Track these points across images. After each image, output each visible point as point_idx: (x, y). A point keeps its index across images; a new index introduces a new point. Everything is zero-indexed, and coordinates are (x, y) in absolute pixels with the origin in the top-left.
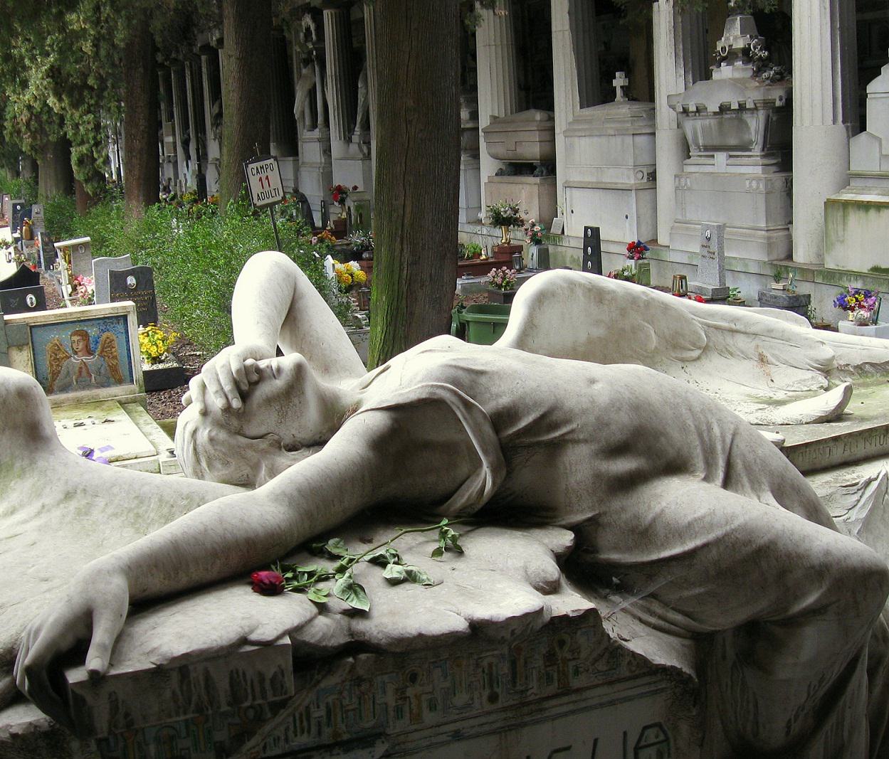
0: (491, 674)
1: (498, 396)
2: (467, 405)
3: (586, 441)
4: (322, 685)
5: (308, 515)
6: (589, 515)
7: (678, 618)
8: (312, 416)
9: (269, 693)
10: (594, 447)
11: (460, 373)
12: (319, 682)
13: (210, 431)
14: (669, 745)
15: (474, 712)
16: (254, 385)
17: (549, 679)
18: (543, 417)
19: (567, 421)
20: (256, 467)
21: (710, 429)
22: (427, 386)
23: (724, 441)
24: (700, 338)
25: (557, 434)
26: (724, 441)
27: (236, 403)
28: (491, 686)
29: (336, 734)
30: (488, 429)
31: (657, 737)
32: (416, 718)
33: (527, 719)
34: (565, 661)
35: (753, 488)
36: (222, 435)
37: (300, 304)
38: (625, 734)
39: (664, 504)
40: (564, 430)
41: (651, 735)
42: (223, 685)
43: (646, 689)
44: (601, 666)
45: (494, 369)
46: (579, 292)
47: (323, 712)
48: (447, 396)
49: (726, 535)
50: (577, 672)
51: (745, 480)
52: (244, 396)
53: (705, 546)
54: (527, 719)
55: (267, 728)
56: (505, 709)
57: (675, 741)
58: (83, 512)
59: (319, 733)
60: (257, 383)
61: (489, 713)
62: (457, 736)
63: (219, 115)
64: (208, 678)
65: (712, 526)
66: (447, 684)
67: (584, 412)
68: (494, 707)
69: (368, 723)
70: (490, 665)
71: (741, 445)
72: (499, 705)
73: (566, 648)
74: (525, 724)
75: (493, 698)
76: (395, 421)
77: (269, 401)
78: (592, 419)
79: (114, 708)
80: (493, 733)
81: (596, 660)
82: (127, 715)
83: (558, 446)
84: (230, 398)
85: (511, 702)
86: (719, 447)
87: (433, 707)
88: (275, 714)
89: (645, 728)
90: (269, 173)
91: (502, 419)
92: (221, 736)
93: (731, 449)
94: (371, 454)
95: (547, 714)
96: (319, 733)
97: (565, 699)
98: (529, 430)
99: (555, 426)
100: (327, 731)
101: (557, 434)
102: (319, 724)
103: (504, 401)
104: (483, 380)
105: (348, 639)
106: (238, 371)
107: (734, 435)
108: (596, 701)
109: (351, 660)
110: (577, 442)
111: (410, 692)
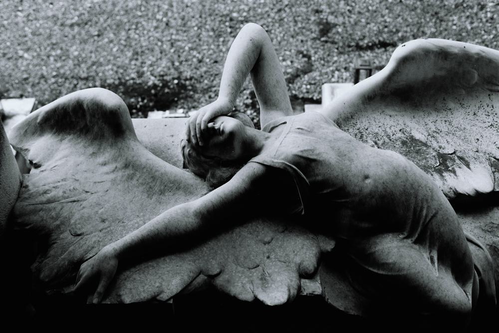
1: (317, 175)
8: (237, 150)
11: (302, 160)
13: (189, 151)
20: (207, 171)
21: (421, 210)
22: (284, 163)
36: (194, 154)
39: (377, 249)
45: (321, 159)
51: (428, 242)
58: (130, 177)
65: (391, 270)
67: (355, 195)
78: (357, 199)
84: (199, 140)
104: (313, 164)
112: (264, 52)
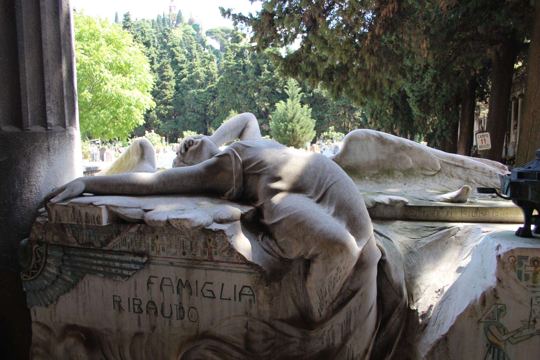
0: (183, 244)
2: (236, 157)
3: (267, 174)
4: (130, 231)
5: (164, 183)
6: (261, 203)
7: (277, 249)
9: (96, 222)
10: (269, 176)
12: (129, 229)
14: (254, 297)
15: (177, 257)
16: (190, 146)
17: (205, 253)
18: (258, 164)
19: (265, 166)
23: (327, 185)
24: (437, 166)
25: (261, 170)
26: (327, 185)
27: (183, 151)
28: (183, 248)
29: (133, 250)
30: (239, 166)
31: (249, 292)
32: (158, 252)
33: (196, 266)
34: (211, 248)
35: (329, 204)
37: (246, 129)
38: (235, 286)
40: (263, 169)
41: (246, 291)
42: (84, 216)
43: (244, 270)
44: (225, 254)
45: (254, 146)
46: (373, 139)
47: (130, 241)
48: (230, 153)
49: (290, 216)
50: (216, 254)
51: (328, 201)
52: (186, 149)
53: (283, 219)
54: (196, 266)
55: (115, 241)
56: (188, 259)
57: (257, 297)
59: (129, 247)
60: (192, 145)
61: (182, 259)
62: (172, 264)
63: (516, 125)
64: (80, 212)
66: (169, 243)
67: (272, 164)
68: (183, 257)
69: (143, 249)
70: (183, 241)
71: (334, 186)
72: (186, 257)
73: (211, 243)
74: (195, 268)
75: (184, 254)
76: (218, 161)
77: (191, 151)
79: (57, 215)
80: (184, 267)
81: (223, 251)
82: (60, 217)
83: (259, 175)
85: (190, 257)
86: (325, 186)
87: (164, 250)
88: (117, 237)
89: (244, 286)
90: (486, 138)
91: (245, 164)
92: (102, 239)
93: (328, 188)
94: (203, 170)
95: (205, 266)
96: (129, 247)
97: (211, 263)
98: (252, 168)
99: (260, 168)
100: (131, 248)
101: (261, 170)
102: (129, 244)
103: (250, 157)
104: (247, 149)
105: (140, 218)
106: (186, 141)
107: (335, 182)
108: (223, 268)
109: (139, 225)
110: (265, 174)
111: (157, 242)
112: (250, 124)
